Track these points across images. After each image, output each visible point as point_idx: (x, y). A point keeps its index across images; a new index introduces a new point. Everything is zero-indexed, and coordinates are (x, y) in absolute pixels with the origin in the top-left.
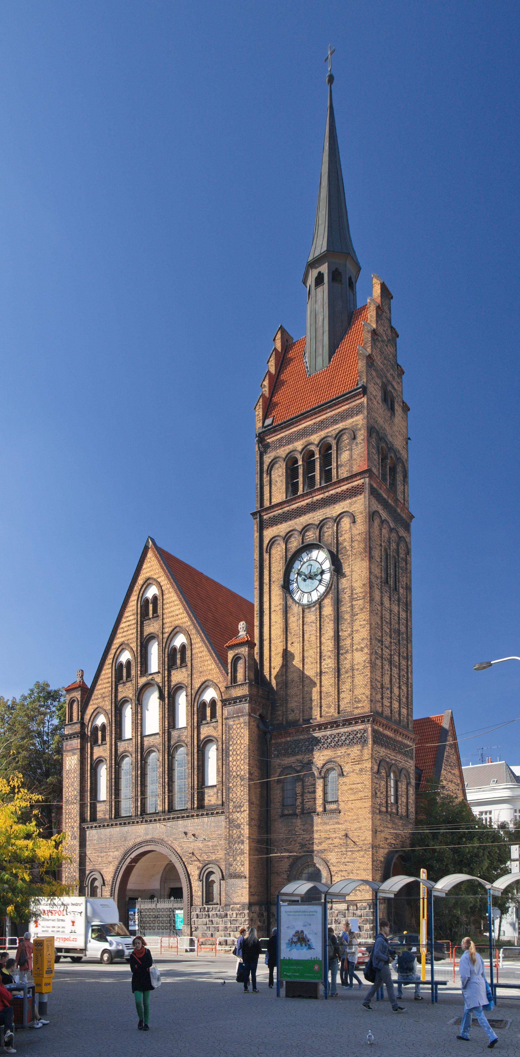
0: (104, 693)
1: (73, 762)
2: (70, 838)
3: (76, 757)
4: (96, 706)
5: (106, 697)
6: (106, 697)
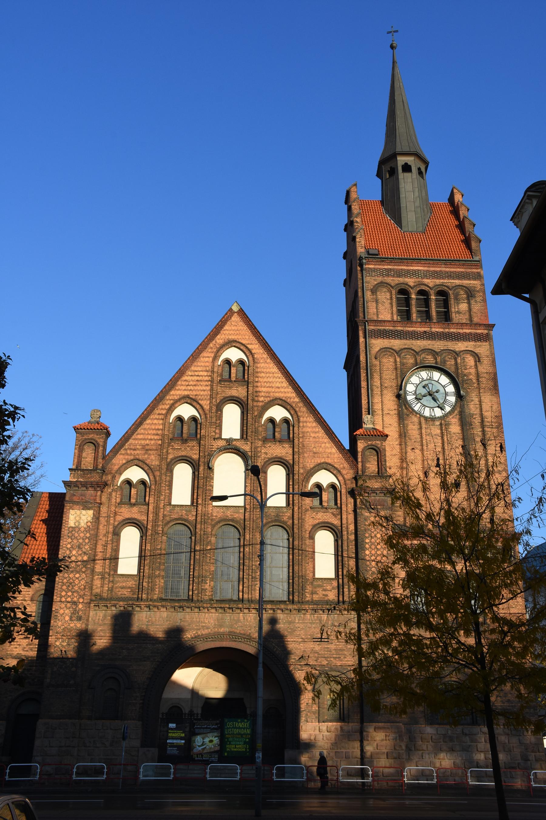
0: (147, 445)
1: (83, 518)
2: (67, 618)
3: (91, 512)
4: (132, 457)
5: (150, 450)
6: (150, 450)
